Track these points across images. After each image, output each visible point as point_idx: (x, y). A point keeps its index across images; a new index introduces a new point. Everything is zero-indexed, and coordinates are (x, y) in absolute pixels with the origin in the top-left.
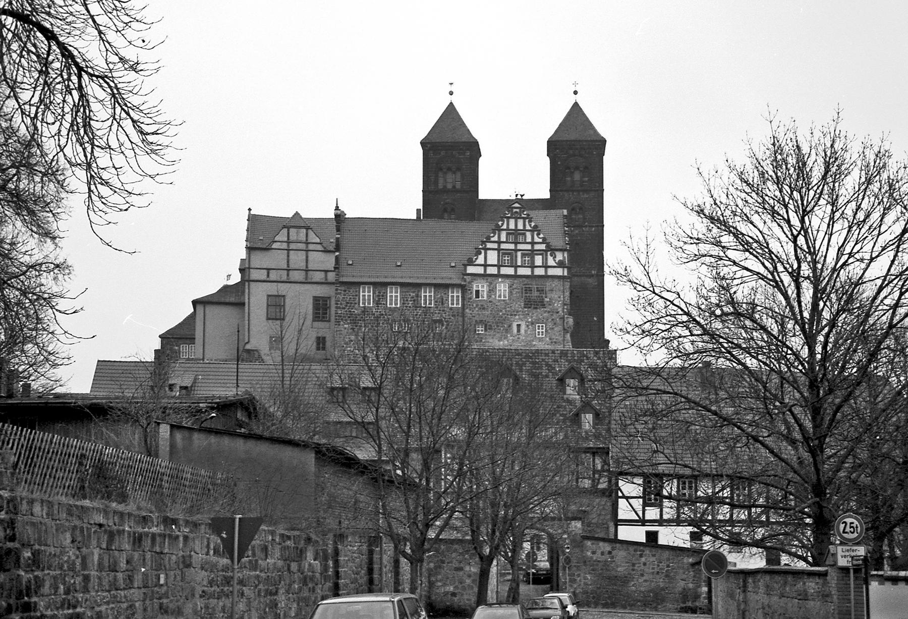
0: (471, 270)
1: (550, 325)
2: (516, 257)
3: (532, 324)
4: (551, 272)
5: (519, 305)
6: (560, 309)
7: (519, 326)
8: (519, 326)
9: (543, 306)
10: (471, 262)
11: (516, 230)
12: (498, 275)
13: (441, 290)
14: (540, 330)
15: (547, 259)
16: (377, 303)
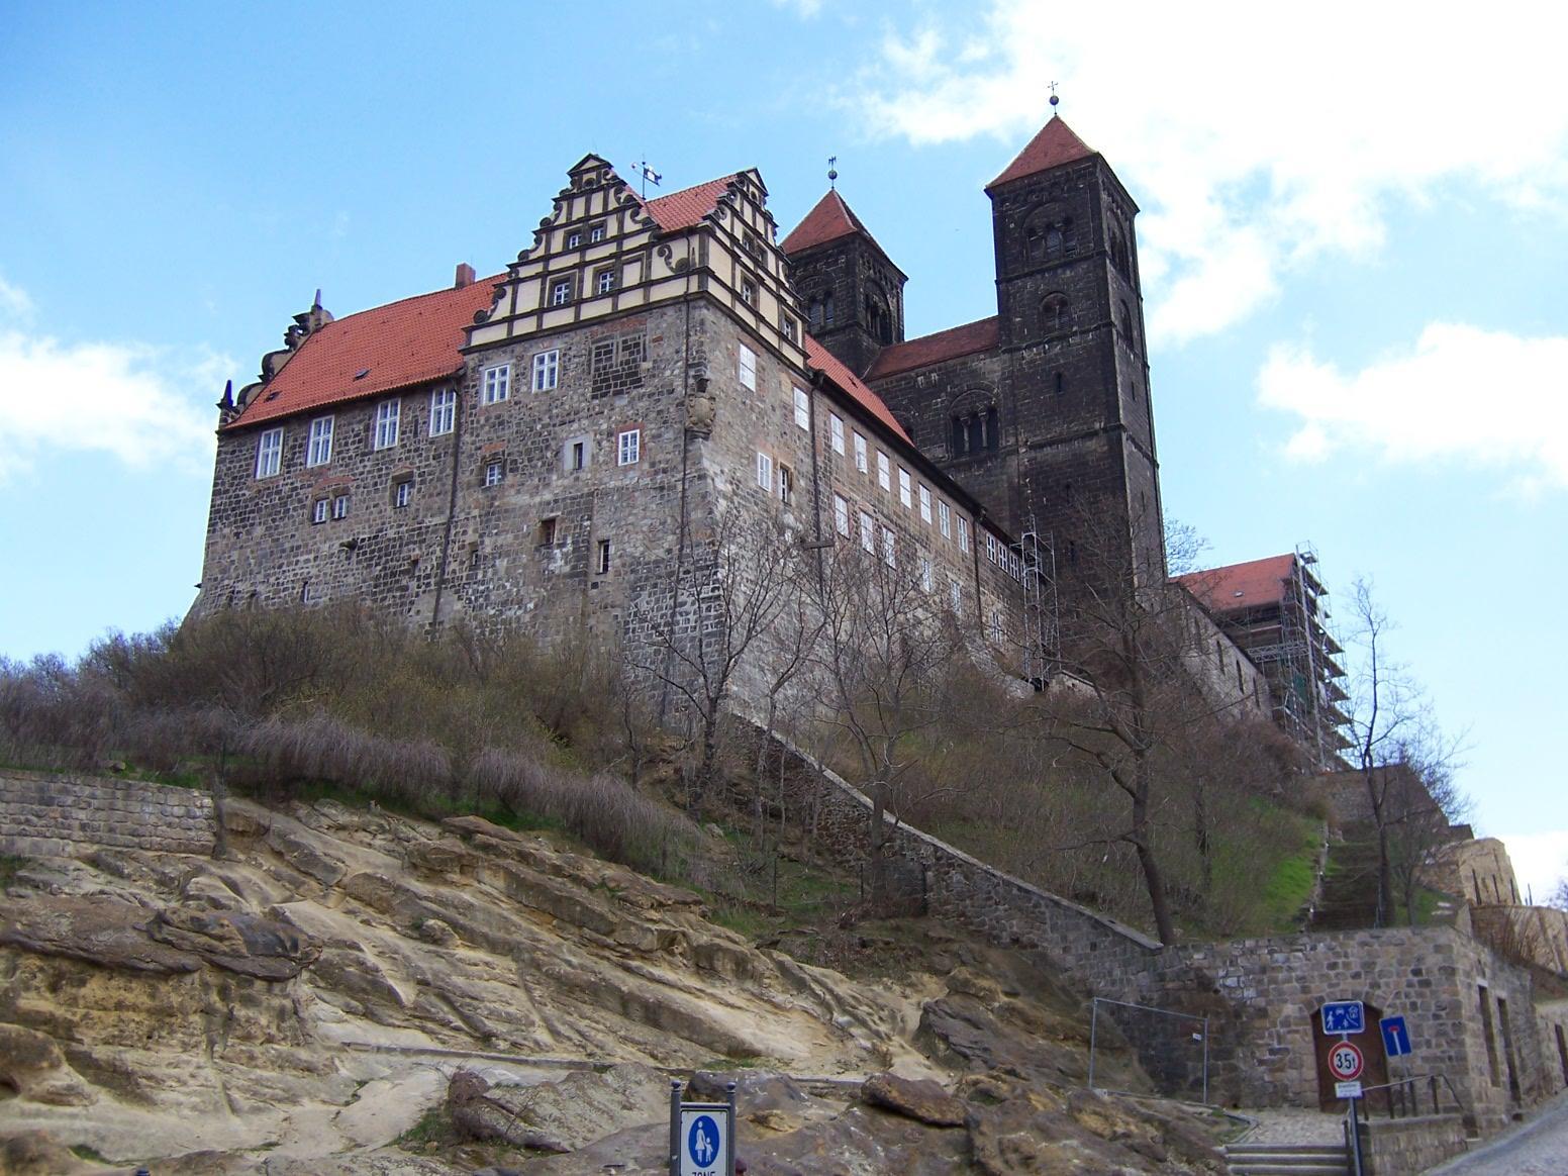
0: (480, 338)
1: (652, 428)
2: (581, 281)
3: (610, 434)
4: (658, 294)
5: (579, 397)
6: (678, 383)
7: (579, 447)
8: (579, 447)
9: (637, 382)
10: (482, 321)
11: (587, 218)
12: (540, 335)
13: (416, 404)
14: (628, 447)
15: (649, 267)
16: (288, 464)
